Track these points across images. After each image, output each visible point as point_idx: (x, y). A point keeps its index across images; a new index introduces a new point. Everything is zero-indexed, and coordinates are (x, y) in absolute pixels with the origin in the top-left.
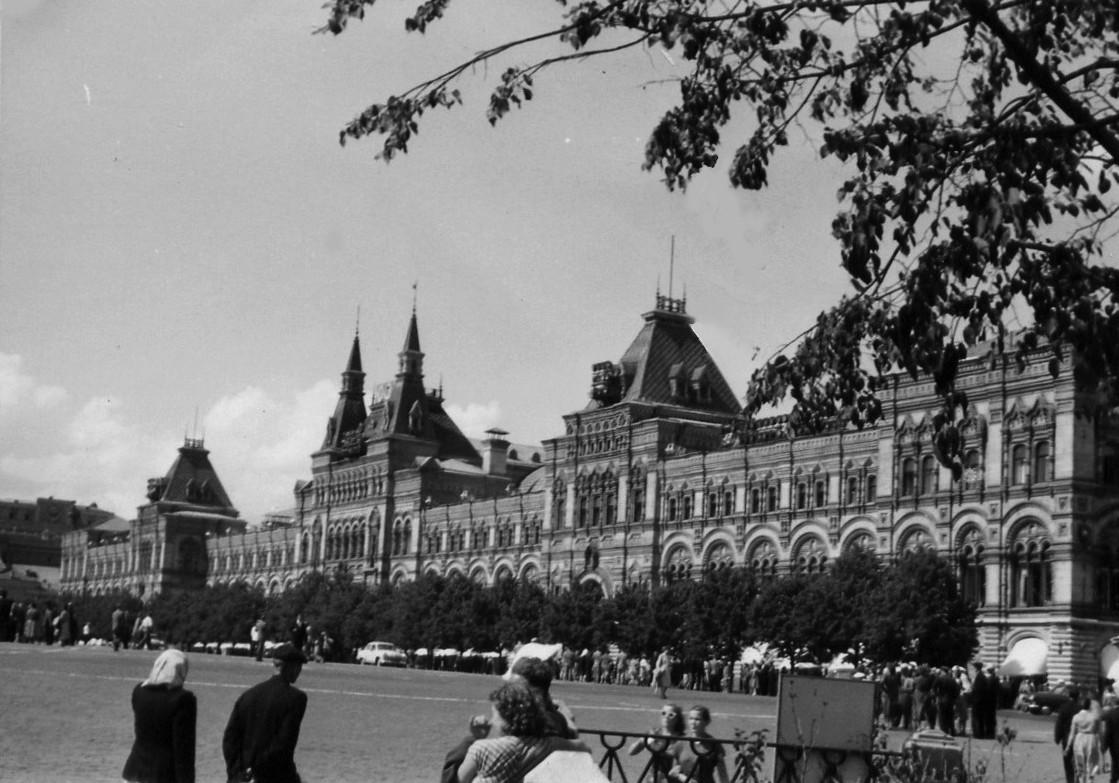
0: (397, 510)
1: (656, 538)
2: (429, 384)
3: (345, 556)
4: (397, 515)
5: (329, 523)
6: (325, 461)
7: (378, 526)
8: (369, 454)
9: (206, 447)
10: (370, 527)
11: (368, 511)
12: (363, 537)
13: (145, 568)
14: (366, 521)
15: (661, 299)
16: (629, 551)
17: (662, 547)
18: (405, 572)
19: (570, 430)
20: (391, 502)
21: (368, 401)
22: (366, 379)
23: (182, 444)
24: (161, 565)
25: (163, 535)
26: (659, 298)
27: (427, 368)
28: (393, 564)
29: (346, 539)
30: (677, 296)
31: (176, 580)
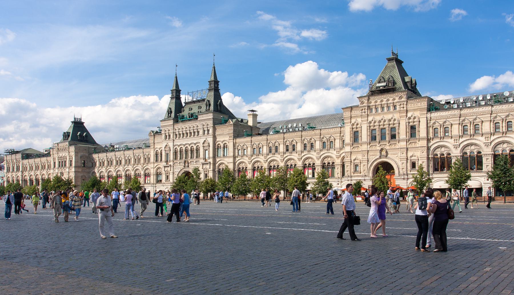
0: (217, 140)
1: (427, 145)
4: (218, 141)
5: (174, 146)
6: (171, 122)
7: (209, 146)
9: (83, 121)
11: (202, 141)
12: (198, 150)
16: (409, 149)
17: (430, 147)
20: (214, 137)
21: (183, 101)
23: (73, 120)
24: (73, 165)
28: (217, 160)
29: (186, 151)
31: (80, 170)
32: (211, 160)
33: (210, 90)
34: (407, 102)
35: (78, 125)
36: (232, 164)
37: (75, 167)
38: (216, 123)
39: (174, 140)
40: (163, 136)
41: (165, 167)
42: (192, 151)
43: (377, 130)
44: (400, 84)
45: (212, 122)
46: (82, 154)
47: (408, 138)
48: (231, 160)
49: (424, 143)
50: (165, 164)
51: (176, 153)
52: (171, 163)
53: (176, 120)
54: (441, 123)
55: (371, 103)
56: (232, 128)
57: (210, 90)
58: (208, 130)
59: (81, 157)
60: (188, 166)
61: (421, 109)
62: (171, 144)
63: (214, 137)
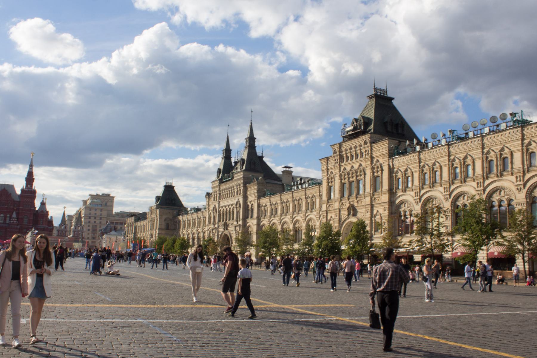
2: (259, 152)
3: (226, 220)
6: (217, 183)
8: (235, 179)
9: (173, 185)
10: (237, 208)
12: (233, 212)
13: (152, 228)
14: (234, 206)
15: (376, 89)
18: (251, 225)
19: (335, 152)
20: (245, 197)
21: (233, 160)
22: (232, 152)
25: (158, 216)
26: (375, 88)
27: (258, 144)
30: (383, 88)
31: (163, 232)
32: (240, 223)
33: (246, 148)
34: (371, 147)
35: (169, 189)
36: (255, 227)
37: (159, 229)
38: (247, 182)
39: (219, 202)
40: (213, 196)
41: (213, 229)
42: (230, 212)
43: (347, 182)
44: (372, 127)
45: (242, 181)
46: (166, 216)
47: (371, 192)
48: (255, 222)
49: (385, 198)
50: (212, 227)
51: (220, 215)
52: (216, 226)
53: (221, 181)
54: (403, 171)
55: (342, 152)
56: (256, 187)
57: (246, 148)
58: (240, 190)
59: (165, 220)
60: (227, 229)
61: (383, 155)
62: (217, 206)
63: (245, 197)
